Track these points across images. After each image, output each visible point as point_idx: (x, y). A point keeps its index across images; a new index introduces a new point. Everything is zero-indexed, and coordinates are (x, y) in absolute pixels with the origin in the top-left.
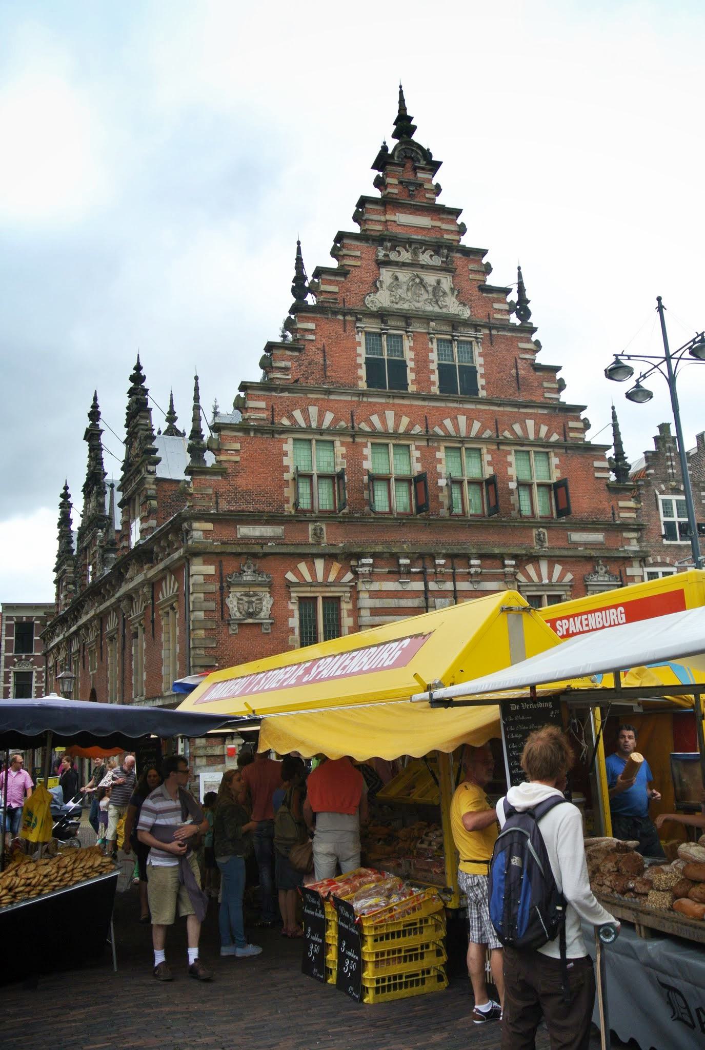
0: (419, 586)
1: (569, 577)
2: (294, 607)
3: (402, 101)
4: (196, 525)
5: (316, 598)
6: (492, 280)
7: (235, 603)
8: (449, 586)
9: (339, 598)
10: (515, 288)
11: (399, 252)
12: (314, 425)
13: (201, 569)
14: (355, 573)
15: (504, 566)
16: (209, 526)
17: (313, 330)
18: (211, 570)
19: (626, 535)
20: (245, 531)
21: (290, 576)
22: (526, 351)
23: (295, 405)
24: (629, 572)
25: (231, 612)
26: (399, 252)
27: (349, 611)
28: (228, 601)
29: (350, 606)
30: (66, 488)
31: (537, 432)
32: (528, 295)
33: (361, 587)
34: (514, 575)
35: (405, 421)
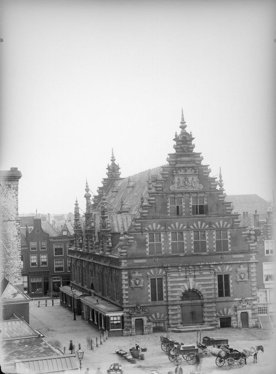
0: (184, 274)
1: (231, 269)
2: (149, 281)
3: (183, 115)
4: (123, 261)
5: (155, 279)
6: (211, 175)
7: (133, 281)
8: (193, 274)
9: (162, 278)
10: (218, 177)
11: (181, 171)
12: (154, 229)
13: (124, 273)
14: (166, 272)
15: (210, 267)
16: (126, 261)
17: (154, 200)
18: (126, 273)
19: (251, 255)
20: (136, 261)
21: (148, 273)
22: (222, 198)
23: (150, 224)
24: (252, 266)
25: (132, 284)
26: (181, 171)
27: (164, 282)
28: (131, 281)
29: (165, 281)
30: (77, 201)
31: (223, 225)
32: (223, 179)
33: (167, 276)
34: (214, 270)
35: (181, 225)
